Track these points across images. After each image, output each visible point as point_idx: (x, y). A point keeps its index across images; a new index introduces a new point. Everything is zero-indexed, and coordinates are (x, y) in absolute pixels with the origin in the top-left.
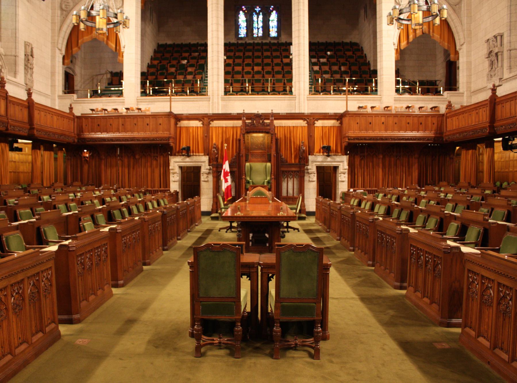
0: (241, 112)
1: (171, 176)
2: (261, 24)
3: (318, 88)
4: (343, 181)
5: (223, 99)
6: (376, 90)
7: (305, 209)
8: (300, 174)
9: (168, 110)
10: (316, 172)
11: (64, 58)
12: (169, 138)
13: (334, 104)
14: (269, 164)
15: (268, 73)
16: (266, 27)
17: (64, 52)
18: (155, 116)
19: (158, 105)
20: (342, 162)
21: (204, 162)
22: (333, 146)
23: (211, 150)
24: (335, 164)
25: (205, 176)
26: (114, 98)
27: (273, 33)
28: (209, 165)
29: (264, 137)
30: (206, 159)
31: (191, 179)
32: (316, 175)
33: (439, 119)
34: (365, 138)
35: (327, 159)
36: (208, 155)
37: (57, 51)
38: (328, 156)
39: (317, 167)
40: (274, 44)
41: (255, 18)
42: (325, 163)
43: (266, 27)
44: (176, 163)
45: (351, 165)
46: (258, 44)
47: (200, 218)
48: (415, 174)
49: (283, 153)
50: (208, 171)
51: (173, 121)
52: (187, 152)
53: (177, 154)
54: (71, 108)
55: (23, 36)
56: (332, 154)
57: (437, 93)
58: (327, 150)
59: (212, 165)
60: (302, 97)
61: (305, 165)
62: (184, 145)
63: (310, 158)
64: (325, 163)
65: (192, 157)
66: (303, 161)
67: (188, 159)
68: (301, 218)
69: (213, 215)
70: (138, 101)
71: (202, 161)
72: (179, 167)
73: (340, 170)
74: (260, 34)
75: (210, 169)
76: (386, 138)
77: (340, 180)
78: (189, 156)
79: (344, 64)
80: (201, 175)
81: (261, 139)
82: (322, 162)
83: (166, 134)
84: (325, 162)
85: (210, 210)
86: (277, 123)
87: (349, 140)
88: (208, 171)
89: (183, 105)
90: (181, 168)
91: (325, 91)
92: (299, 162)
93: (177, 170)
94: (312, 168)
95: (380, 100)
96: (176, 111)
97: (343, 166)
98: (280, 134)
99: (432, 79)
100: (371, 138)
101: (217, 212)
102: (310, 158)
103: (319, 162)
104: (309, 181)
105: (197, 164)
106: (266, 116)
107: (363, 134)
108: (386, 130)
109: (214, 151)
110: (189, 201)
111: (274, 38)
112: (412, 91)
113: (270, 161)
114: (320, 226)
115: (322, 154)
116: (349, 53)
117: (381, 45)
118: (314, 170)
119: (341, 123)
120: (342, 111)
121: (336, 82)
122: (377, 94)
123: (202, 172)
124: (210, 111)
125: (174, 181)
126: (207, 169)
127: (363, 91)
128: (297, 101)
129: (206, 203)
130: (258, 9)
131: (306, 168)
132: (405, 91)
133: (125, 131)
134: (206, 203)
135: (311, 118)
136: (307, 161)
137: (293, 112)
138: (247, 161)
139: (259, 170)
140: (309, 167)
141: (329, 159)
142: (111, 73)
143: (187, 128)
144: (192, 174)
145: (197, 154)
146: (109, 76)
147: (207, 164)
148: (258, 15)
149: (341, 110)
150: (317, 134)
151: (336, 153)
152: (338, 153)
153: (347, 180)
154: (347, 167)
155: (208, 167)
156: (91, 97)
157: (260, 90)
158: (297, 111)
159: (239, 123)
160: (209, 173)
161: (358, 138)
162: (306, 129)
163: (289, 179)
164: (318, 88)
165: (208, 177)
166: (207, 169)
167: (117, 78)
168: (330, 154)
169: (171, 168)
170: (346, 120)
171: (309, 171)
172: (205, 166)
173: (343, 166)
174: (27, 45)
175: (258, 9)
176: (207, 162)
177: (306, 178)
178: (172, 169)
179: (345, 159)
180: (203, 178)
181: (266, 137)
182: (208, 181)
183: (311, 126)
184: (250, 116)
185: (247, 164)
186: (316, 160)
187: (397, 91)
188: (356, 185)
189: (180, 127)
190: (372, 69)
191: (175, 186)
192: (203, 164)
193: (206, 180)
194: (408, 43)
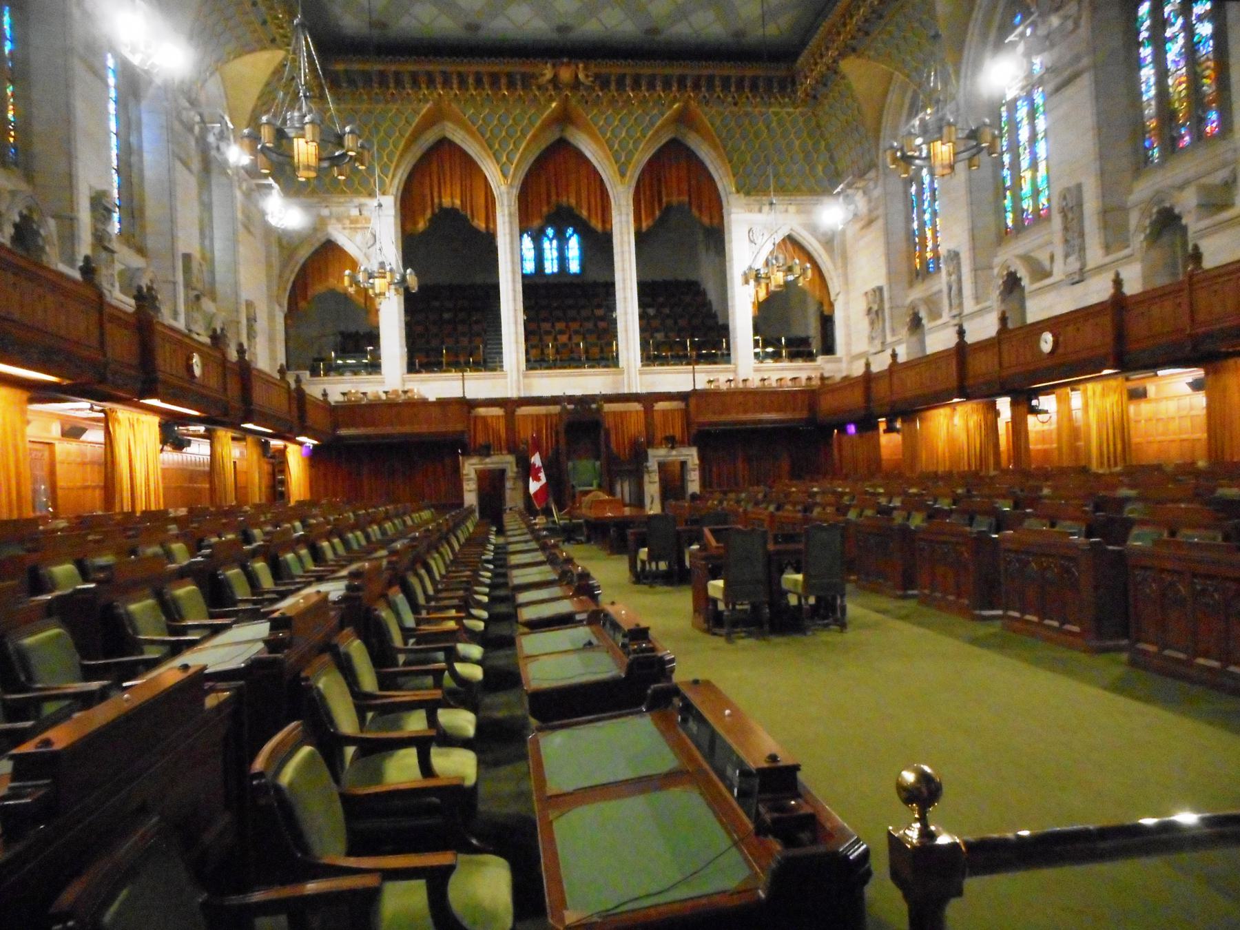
0: (561, 394)
2: (555, 254)
3: (653, 355)
5: (525, 376)
6: (729, 355)
8: (637, 474)
9: (461, 395)
11: (286, 317)
12: (463, 432)
13: (676, 379)
14: (598, 463)
15: (577, 332)
16: (563, 260)
17: (286, 309)
18: (443, 403)
19: (438, 386)
20: (691, 455)
22: (678, 435)
24: (682, 458)
26: (364, 377)
27: (574, 267)
31: (492, 484)
33: (810, 396)
34: (716, 424)
37: (277, 308)
38: (673, 448)
40: (578, 285)
41: (546, 244)
43: (563, 260)
44: (470, 468)
45: (702, 458)
46: (555, 285)
48: (785, 464)
49: (613, 445)
51: (465, 409)
52: (485, 451)
54: (325, 395)
55: (245, 295)
57: (810, 357)
58: (672, 442)
60: (633, 370)
62: (481, 439)
63: (651, 452)
66: (638, 455)
67: (488, 460)
70: (404, 381)
71: (506, 461)
73: (690, 465)
74: (556, 270)
76: (745, 423)
78: (488, 455)
79: (681, 316)
83: (459, 427)
86: (608, 407)
89: (477, 386)
91: (664, 361)
93: (473, 475)
94: (653, 464)
95: (735, 371)
96: (469, 396)
99: (803, 335)
100: (725, 424)
102: (651, 452)
106: (592, 398)
107: (715, 418)
108: (746, 412)
111: (575, 275)
112: (776, 356)
113: (597, 458)
116: (687, 299)
117: (733, 297)
118: (656, 467)
119: (687, 405)
120: (689, 388)
121: (671, 346)
122: (728, 362)
124: (512, 393)
127: (711, 359)
128: (626, 375)
130: (550, 232)
132: (767, 355)
133: (402, 424)
135: (648, 400)
136: (645, 458)
137: (621, 391)
138: (569, 459)
139: (584, 470)
141: (674, 453)
142: (342, 334)
143: (484, 418)
146: (339, 338)
148: (551, 240)
149: (688, 387)
150: (658, 419)
151: (683, 444)
154: (697, 462)
155: (515, 469)
156: (325, 375)
157: (568, 360)
158: (626, 391)
159: (555, 409)
160: (515, 479)
161: (711, 424)
162: (642, 416)
164: (653, 355)
167: (359, 344)
170: (693, 401)
174: (249, 304)
175: (550, 232)
177: (646, 478)
180: (509, 484)
182: (513, 489)
183: (649, 410)
184: (571, 399)
185: (570, 464)
186: (657, 455)
187: (756, 355)
189: (476, 417)
190: (720, 322)
191: (470, 498)
194: (768, 292)
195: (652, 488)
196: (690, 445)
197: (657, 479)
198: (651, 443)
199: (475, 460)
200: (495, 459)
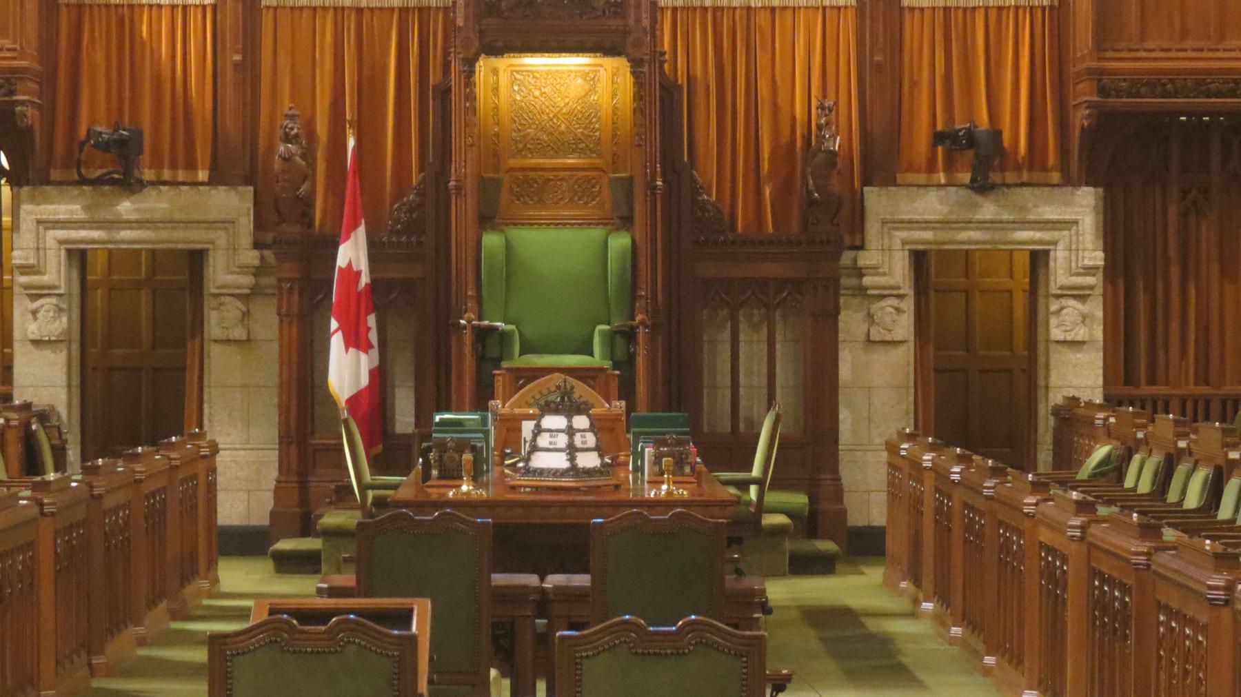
1: (20, 307)
4: (1076, 344)
7: (843, 513)
10: (908, 290)
14: (620, 242)
20: (1070, 229)
21: (227, 224)
23: (271, 149)
25: (234, 309)
28: (257, 245)
29: (591, 78)
30: (233, 204)
32: (908, 305)
34: (1200, 83)
35: (976, 207)
36: (247, 182)
38: (981, 187)
39: (919, 259)
42: (964, 235)
47: (212, 564)
49: (708, 171)
50: (248, 280)
52: (117, 164)
53: (55, 174)
56: (1010, 177)
59: (276, 243)
61: (838, 247)
62: (95, 119)
63: (876, 200)
64: (964, 235)
65: (150, 192)
66: (824, 224)
67: (126, 207)
68: (805, 565)
69: (284, 545)
71: (218, 219)
72: (69, 251)
73: (1060, 273)
75: (258, 272)
77: (1056, 334)
78: (129, 184)
80: (208, 303)
81: (577, 87)
82: (945, 224)
84: (968, 224)
85: (261, 518)
87: (1103, 92)
88: (248, 280)
90: (79, 257)
92: (805, 225)
93: (56, 272)
94: (885, 261)
97: (1073, 249)
98: (692, 60)
101: (306, 529)
102: (876, 200)
103: (925, 225)
104: (869, 341)
105: (179, 234)
109: (287, 159)
110: (150, 461)
113: (626, 222)
114: (901, 593)
115: (942, 177)
118: (899, 272)
123: (211, 288)
125: (37, 343)
126: (243, 269)
129: (243, 471)
131: (847, 257)
134: (243, 471)
138: (487, 220)
140: (866, 259)
141: (988, 209)
144: (145, 297)
145: (181, 175)
147: (246, 240)
152: (1045, 168)
153: (1099, 334)
154: (1097, 258)
155: (251, 257)
161: (1157, 83)
163: (743, 327)
165: (246, 315)
166: (243, 269)
168: (995, 177)
169: (18, 257)
171: (867, 281)
172: (233, 248)
173: (1073, 249)
176: (246, 224)
177: (851, 322)
178: (27, 269)
179: (1082, 208)
180: (220, 320)
181: (604, 76)
185: (492, 241)
186: (911, 216)
188: (1160, 373)
192: (221, 238)
193: (239, 333)
195: (878, 379)
196: (1069, 181)
197: (904, 327)
198: (881, 161)
199: (67, 207)
200: (157, 202)
